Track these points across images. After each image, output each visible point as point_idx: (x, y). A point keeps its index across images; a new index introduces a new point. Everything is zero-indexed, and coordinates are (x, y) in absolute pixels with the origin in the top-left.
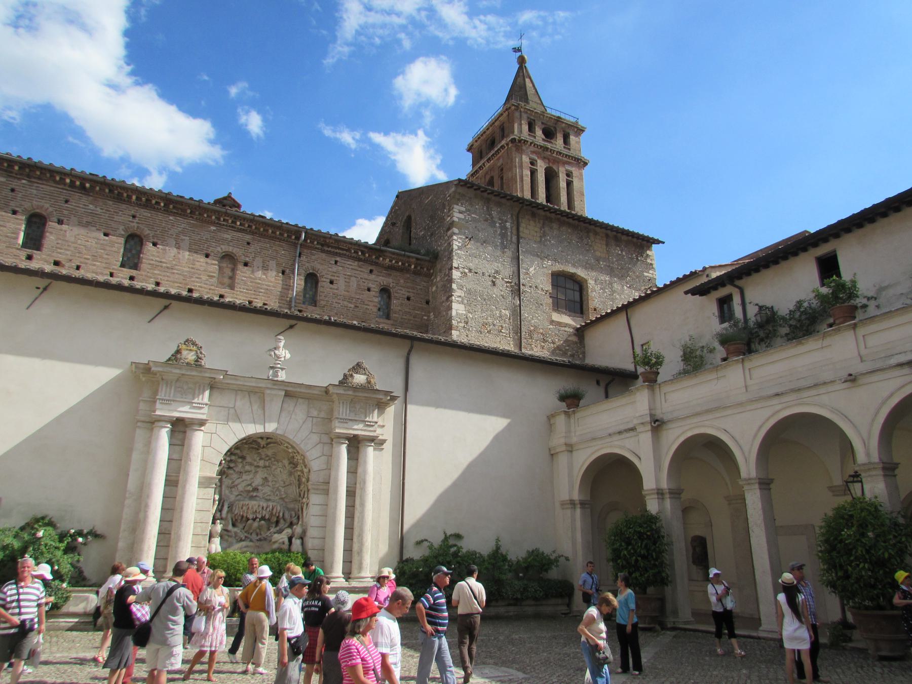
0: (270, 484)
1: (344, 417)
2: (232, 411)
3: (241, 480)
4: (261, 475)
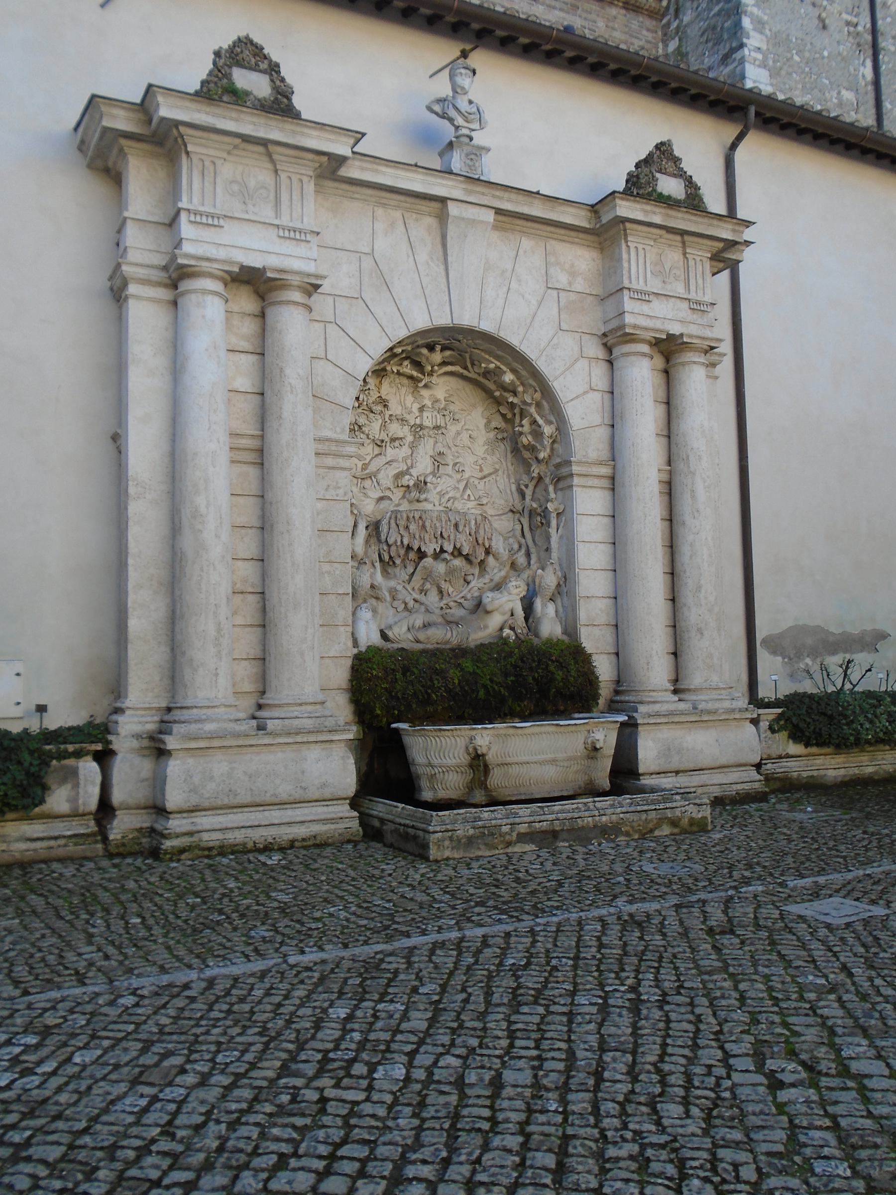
2: (367, 263)
3: (381, 460)
4: (426, 449)
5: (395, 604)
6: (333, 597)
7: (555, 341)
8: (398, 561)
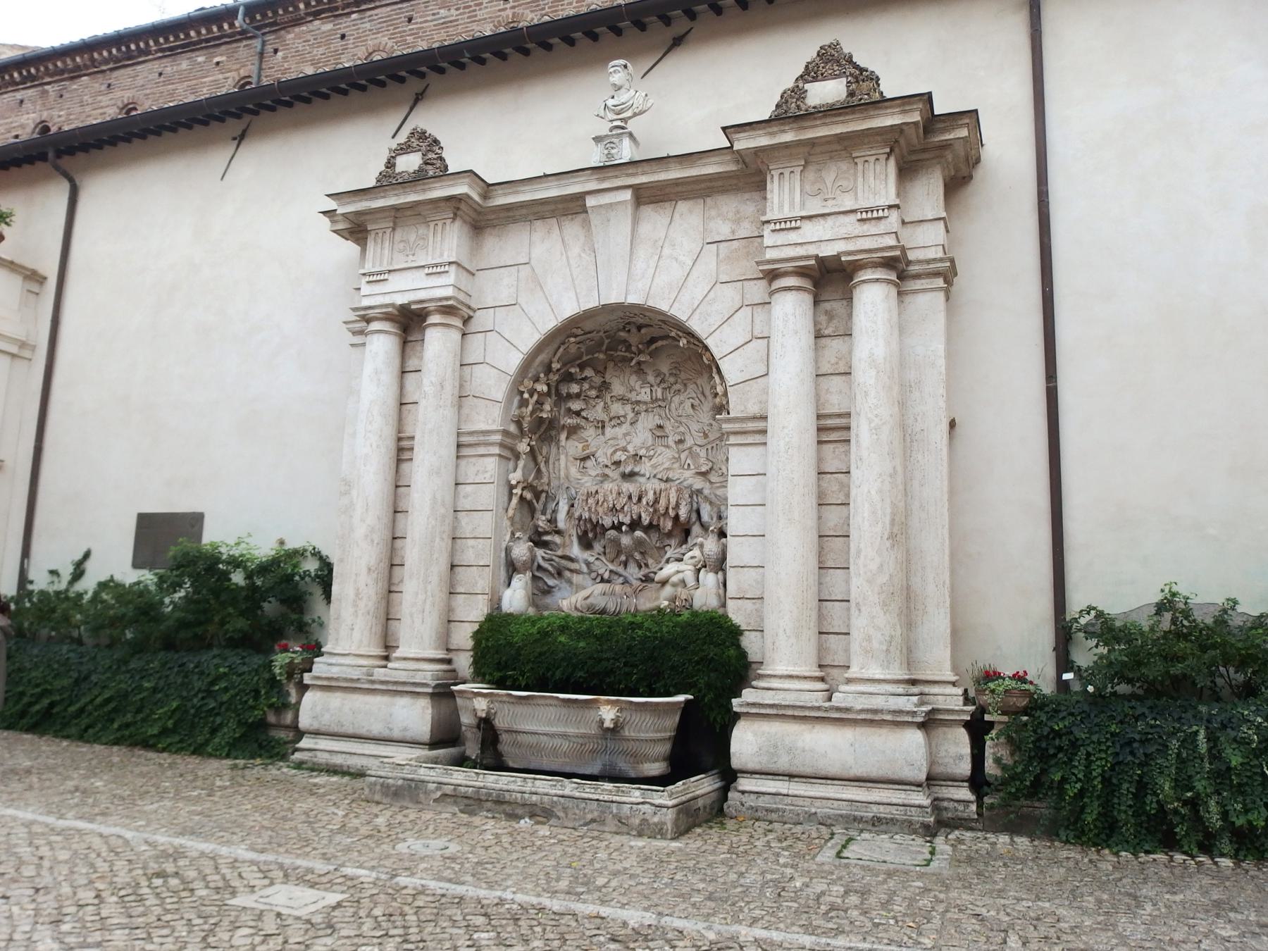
1: (787, 213)
4: (648, 421)
5: (594, 575)
8: (590, 535)
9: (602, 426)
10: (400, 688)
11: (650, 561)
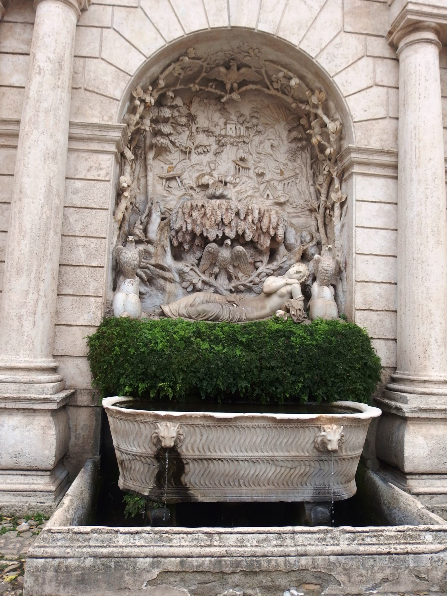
0: (251, 173)
4: (230, 154)
5: (185, 284)
6: (86, 269)
7: (337, 40)
8: (186, 247)
9: (186, 152)
10: (9, 405)
11: (240, 275)
